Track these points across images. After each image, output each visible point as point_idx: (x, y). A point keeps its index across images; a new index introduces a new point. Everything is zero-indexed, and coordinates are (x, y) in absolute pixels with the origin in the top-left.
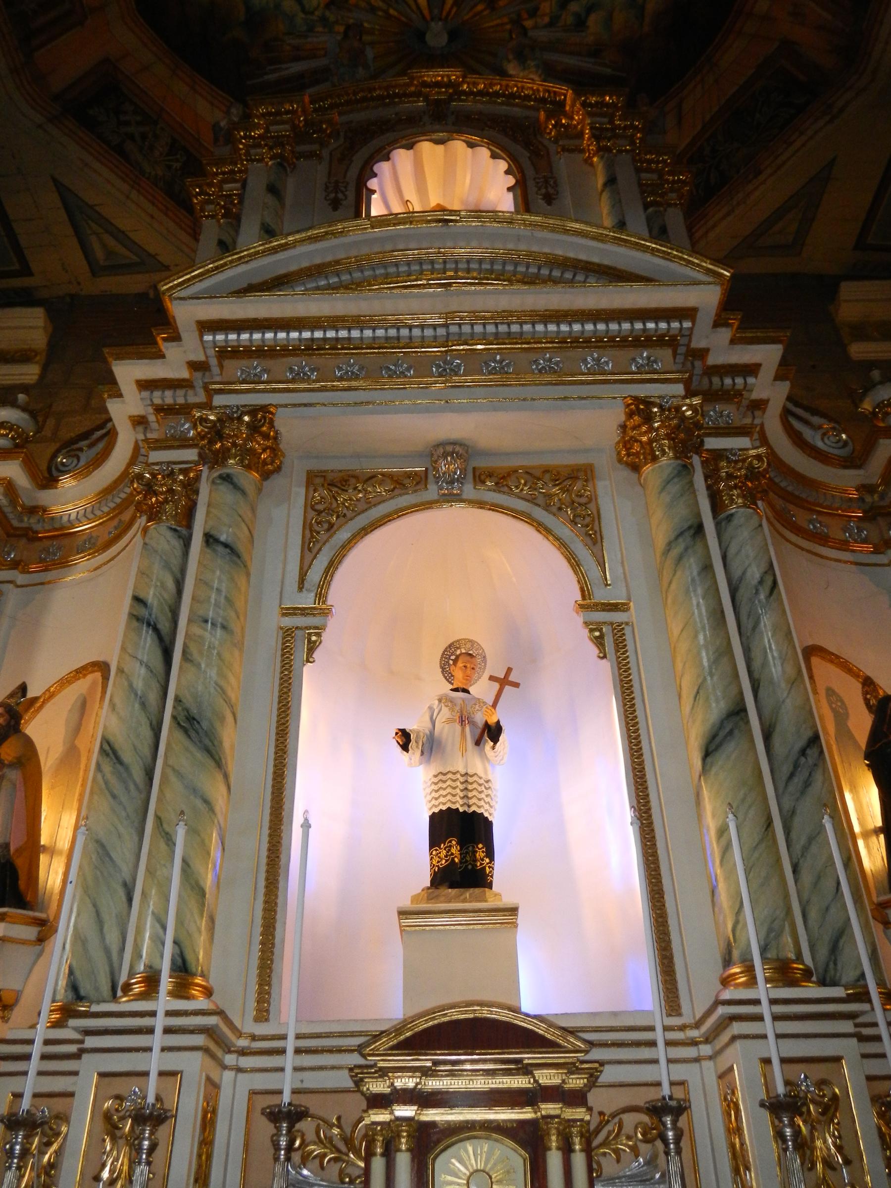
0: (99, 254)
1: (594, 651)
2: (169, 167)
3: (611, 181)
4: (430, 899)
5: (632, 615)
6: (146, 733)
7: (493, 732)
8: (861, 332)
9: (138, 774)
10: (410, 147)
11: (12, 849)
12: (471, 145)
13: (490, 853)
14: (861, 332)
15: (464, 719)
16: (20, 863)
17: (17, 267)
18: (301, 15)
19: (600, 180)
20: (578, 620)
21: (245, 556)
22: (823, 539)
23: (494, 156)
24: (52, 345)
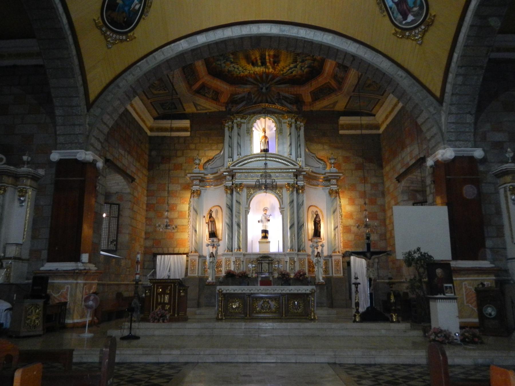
0: (199, 108)
1: (280, 214)
2: (212, 95)
3: (290, 134)
4: (262, 240)
5: (285, 209)
6: (231, 222)
7: (269, 220)
8: (343, 127)
9: (231, 227)
10: (259, 119)
11: (215, 231)
12: (269, 119)
13: (268, 234)
14: (343, 127)
15: (266, 218)
16: (216, 233)
17: (183, 110)
18: (238, 71)
19: (288, 134)
20: (279, 209)
21: (241, 203)
22: (318, 185)
23: (273, 122)
24: (191, 126)
